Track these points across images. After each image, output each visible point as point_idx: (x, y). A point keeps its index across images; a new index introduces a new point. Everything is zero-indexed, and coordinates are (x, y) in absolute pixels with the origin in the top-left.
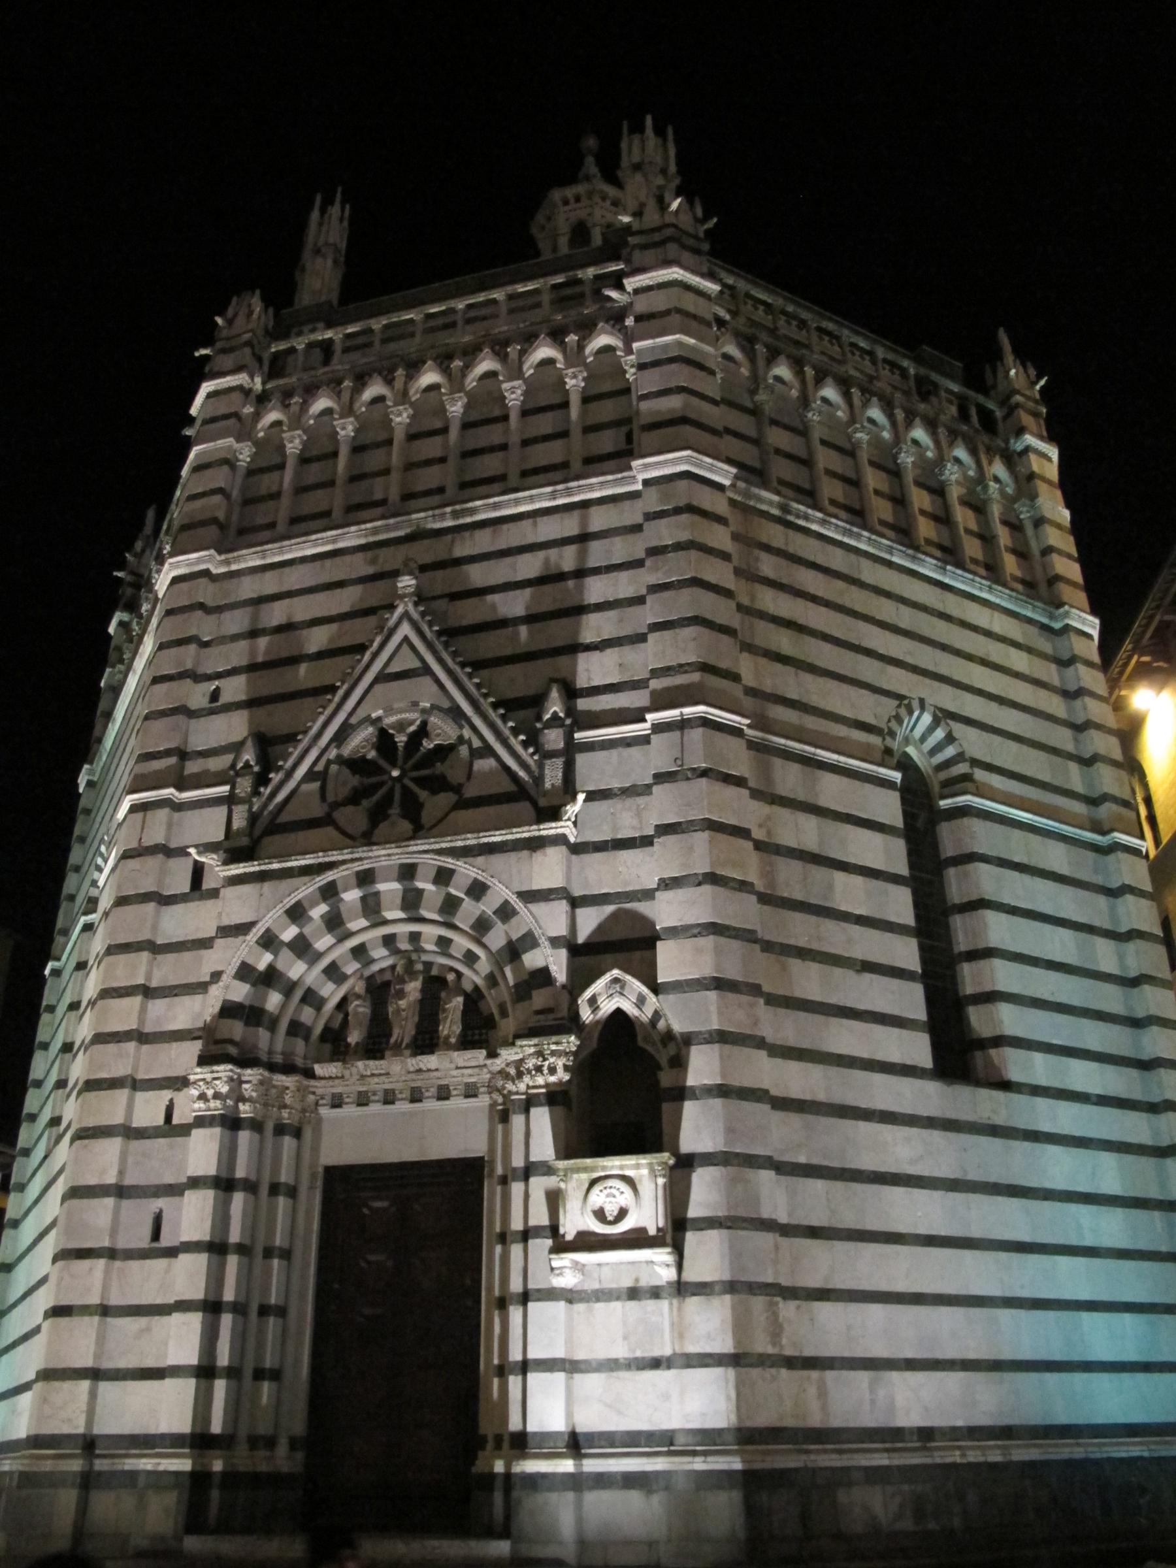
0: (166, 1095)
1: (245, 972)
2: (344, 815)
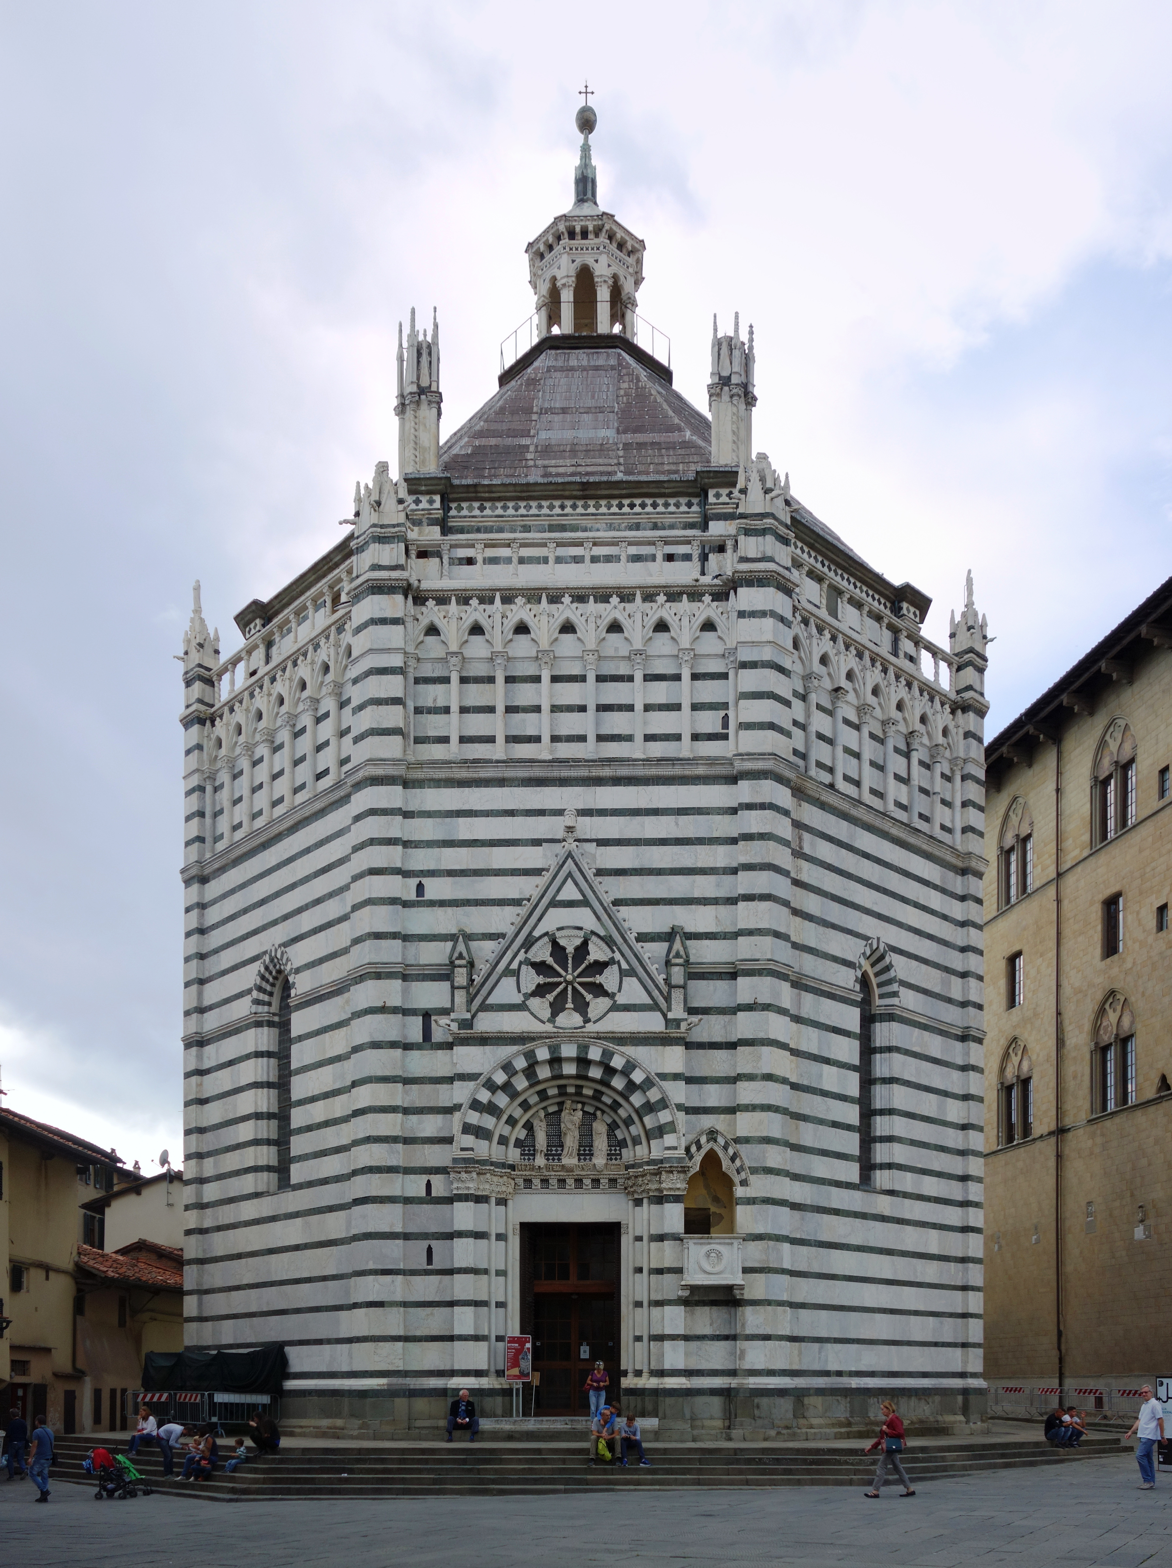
0: (424, 1178)
1: (475, 1105)
2: (535, 1003)
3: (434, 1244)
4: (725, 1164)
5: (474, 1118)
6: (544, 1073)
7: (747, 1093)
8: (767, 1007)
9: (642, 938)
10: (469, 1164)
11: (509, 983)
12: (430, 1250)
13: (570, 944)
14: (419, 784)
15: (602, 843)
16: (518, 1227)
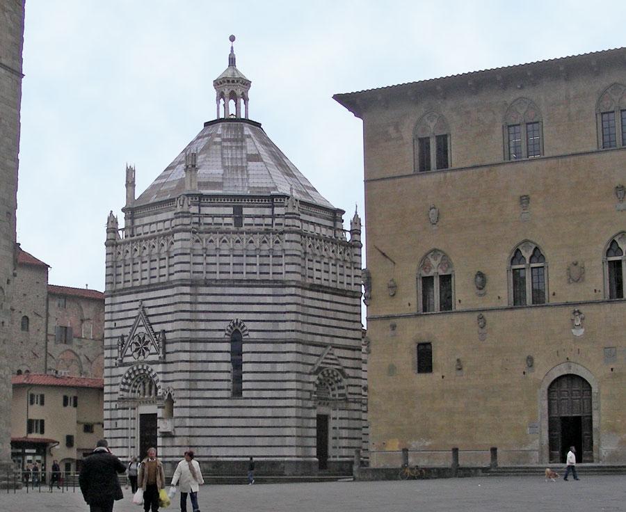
0: (115, 403)
5: (122, 386)
6: (137, 373)
7: (176, 376)
8: (180, 351)
9: (155, 334)
10: (122, 399)
11: (129, 349)
13: (141, 337)
14: (116, 296)
15: (150, 307)
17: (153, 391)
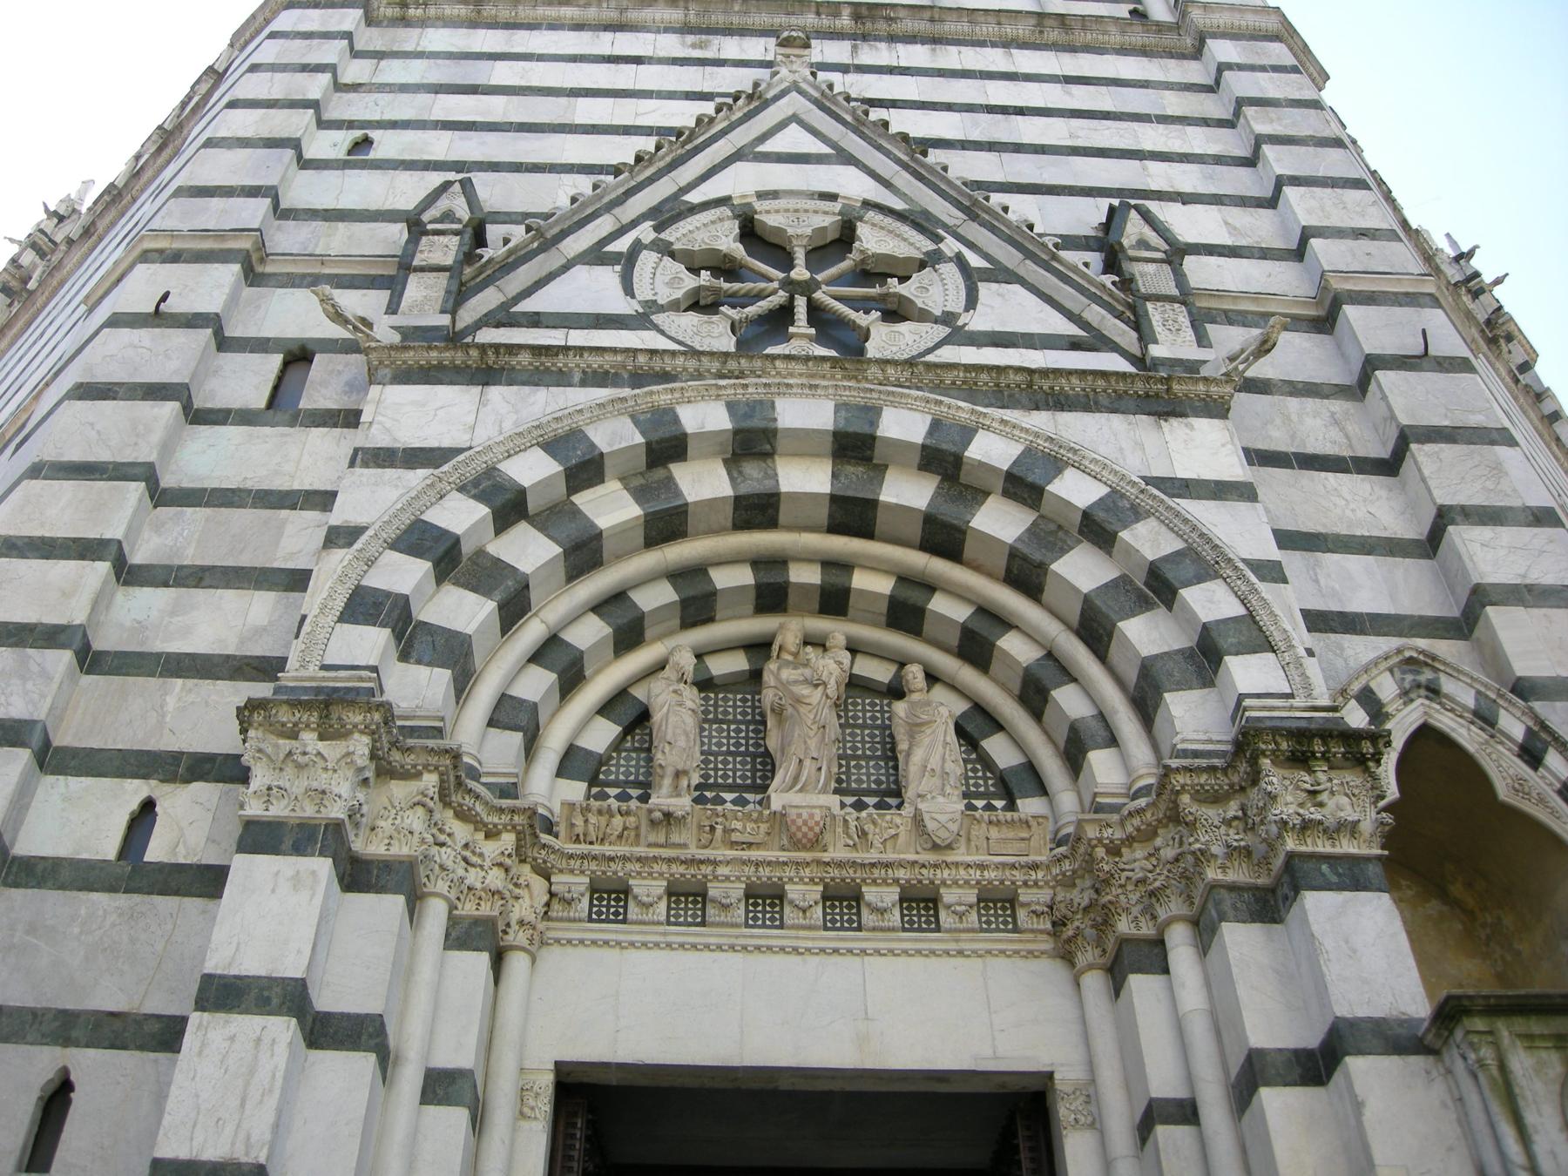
1: (419, 539)
3: (87, 1064)
4: (1504, 771)
5: (404, 574)
6: (703, 482)
12: (57, 1100)
16: (547, 1080)
17: (932, 756)
